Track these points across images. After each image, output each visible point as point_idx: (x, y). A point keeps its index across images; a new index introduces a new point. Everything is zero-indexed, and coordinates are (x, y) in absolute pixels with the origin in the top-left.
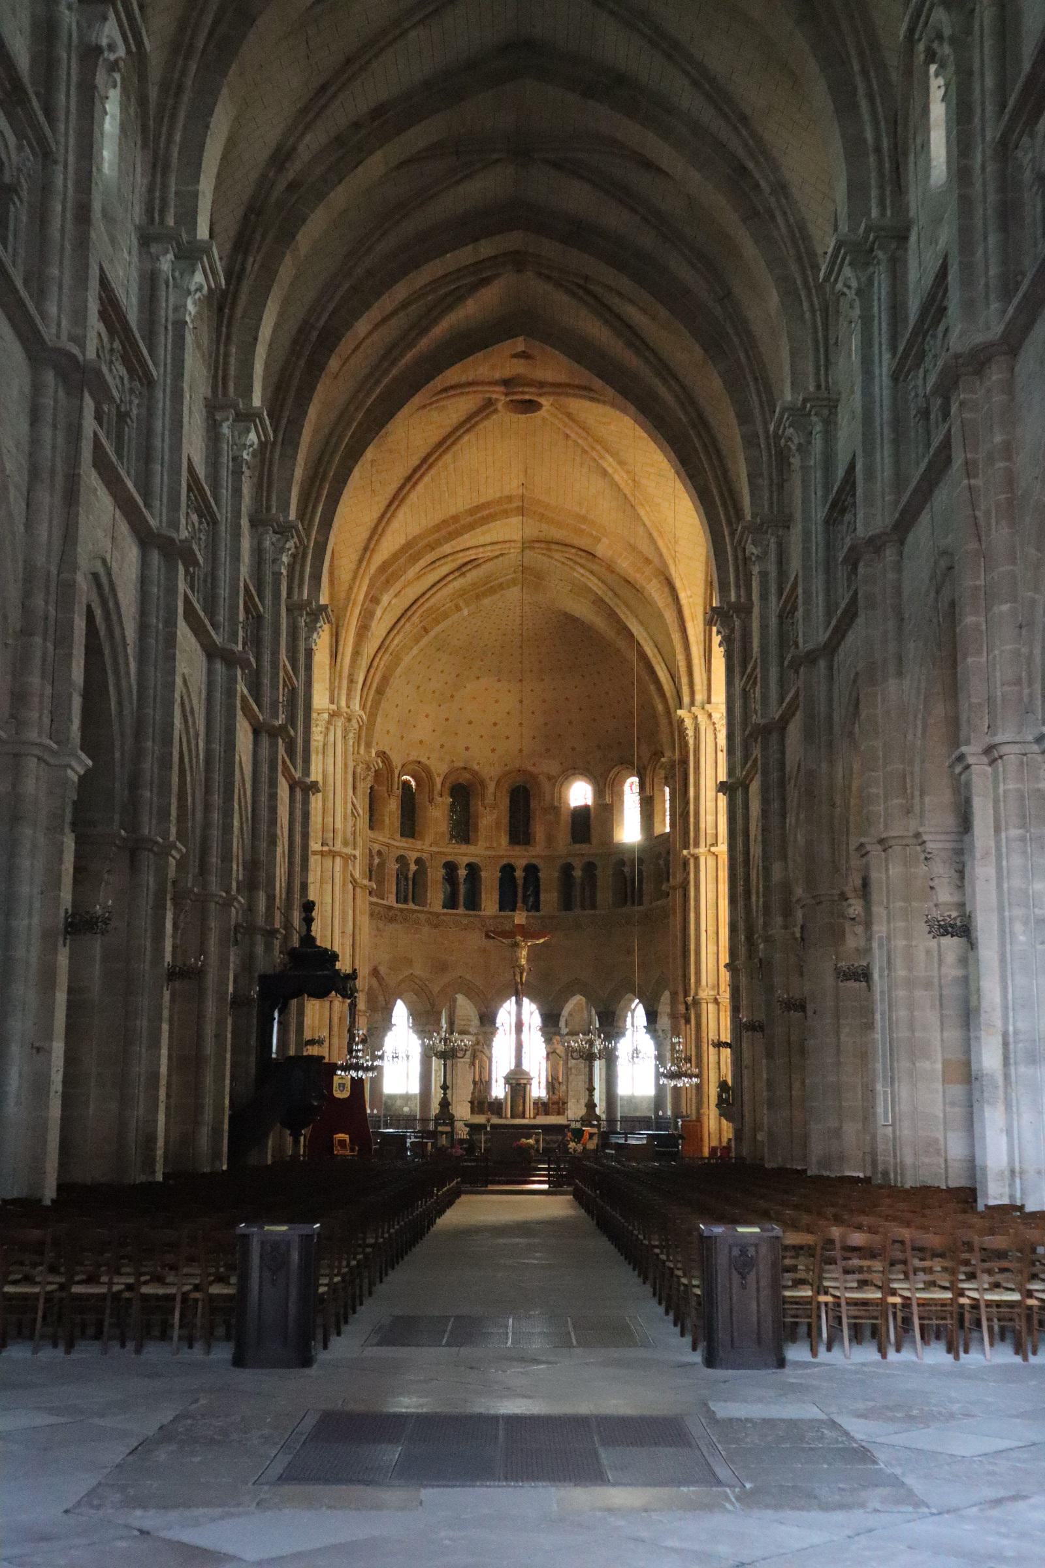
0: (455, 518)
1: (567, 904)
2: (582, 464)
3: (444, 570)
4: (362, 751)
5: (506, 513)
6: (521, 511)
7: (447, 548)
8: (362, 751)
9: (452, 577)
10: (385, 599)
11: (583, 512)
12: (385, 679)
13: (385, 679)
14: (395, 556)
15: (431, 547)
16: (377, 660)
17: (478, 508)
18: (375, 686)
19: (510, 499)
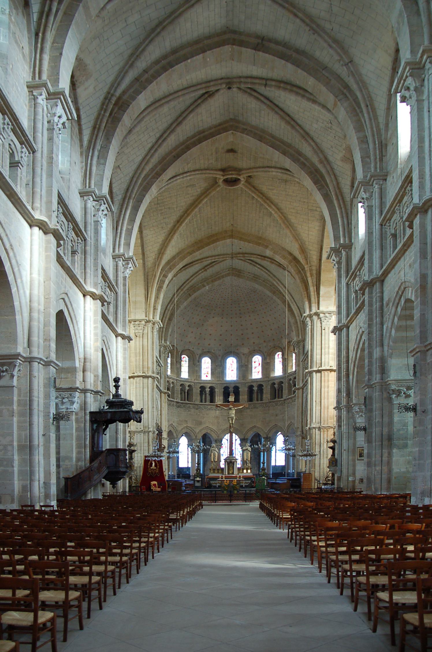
0: (201, 241)
1: (250, 399)
2: (260, 212)
3: (196, 267)
4: (163, 342)
5: (224, 238)
6: (232, 237)
7: (198, 255)
8: (163, 342)
9: (201, 272)
10: (170, 276)
11: (260, 235)
12: (172, 315)
13: (172, 315)
14: (174, 258)
15: (190, 253)
16: (169, 307)
17: (212, 236)
18: (168, 317)
19: (226, 232)
